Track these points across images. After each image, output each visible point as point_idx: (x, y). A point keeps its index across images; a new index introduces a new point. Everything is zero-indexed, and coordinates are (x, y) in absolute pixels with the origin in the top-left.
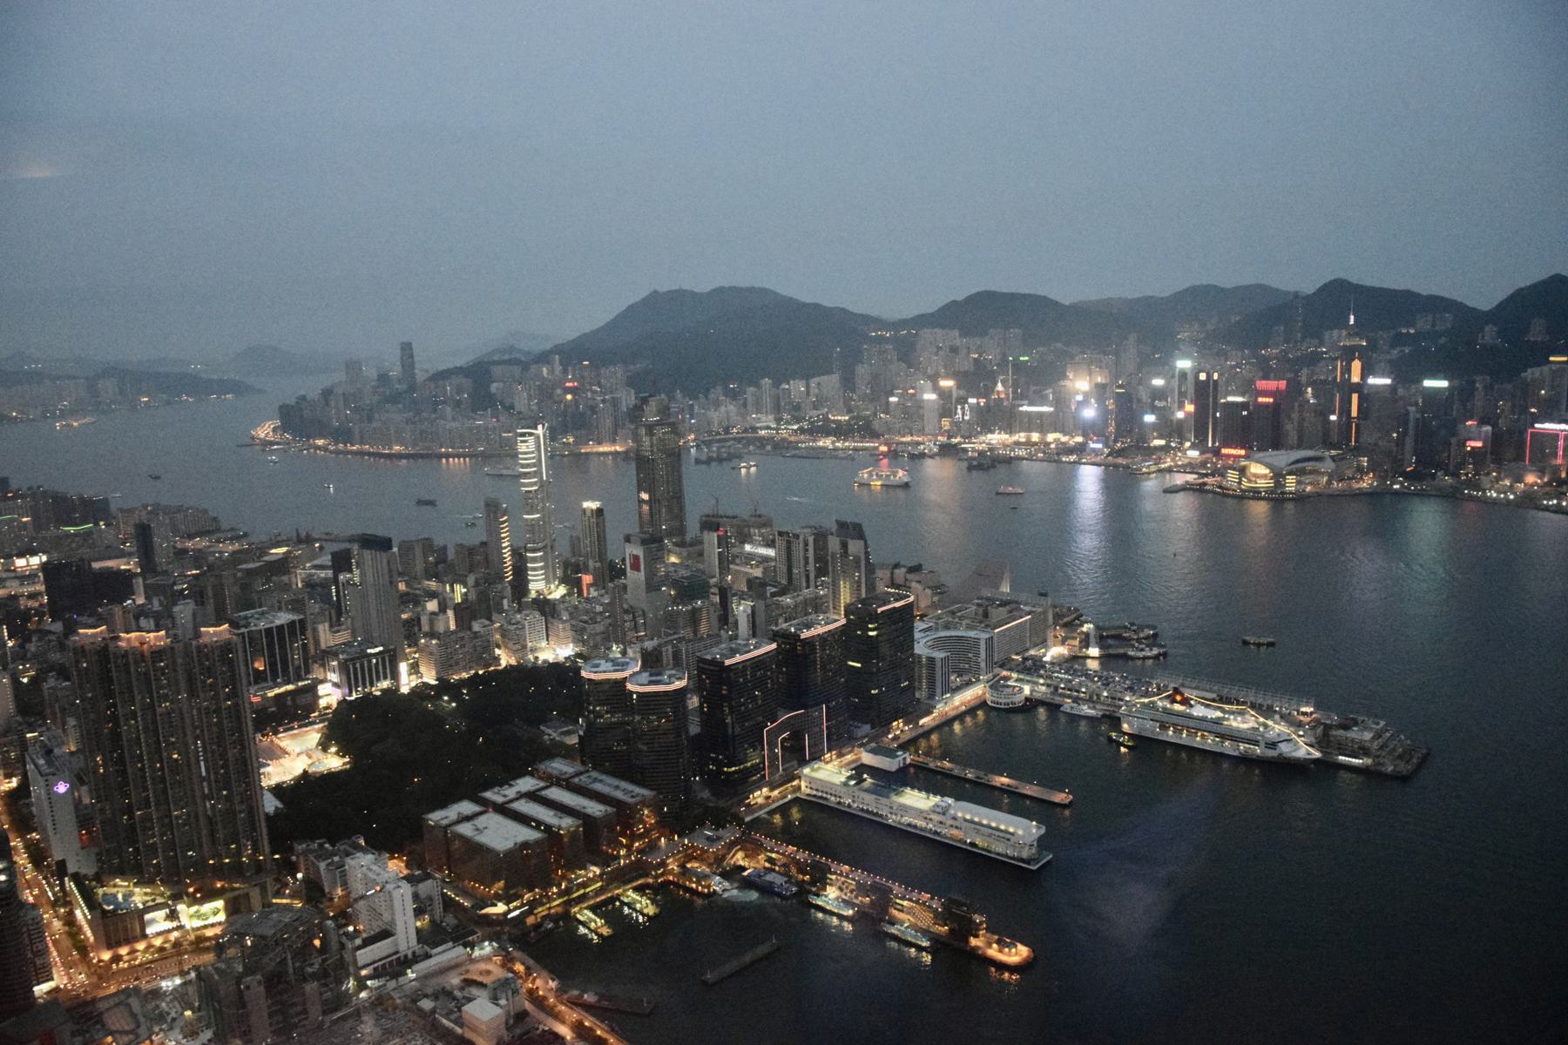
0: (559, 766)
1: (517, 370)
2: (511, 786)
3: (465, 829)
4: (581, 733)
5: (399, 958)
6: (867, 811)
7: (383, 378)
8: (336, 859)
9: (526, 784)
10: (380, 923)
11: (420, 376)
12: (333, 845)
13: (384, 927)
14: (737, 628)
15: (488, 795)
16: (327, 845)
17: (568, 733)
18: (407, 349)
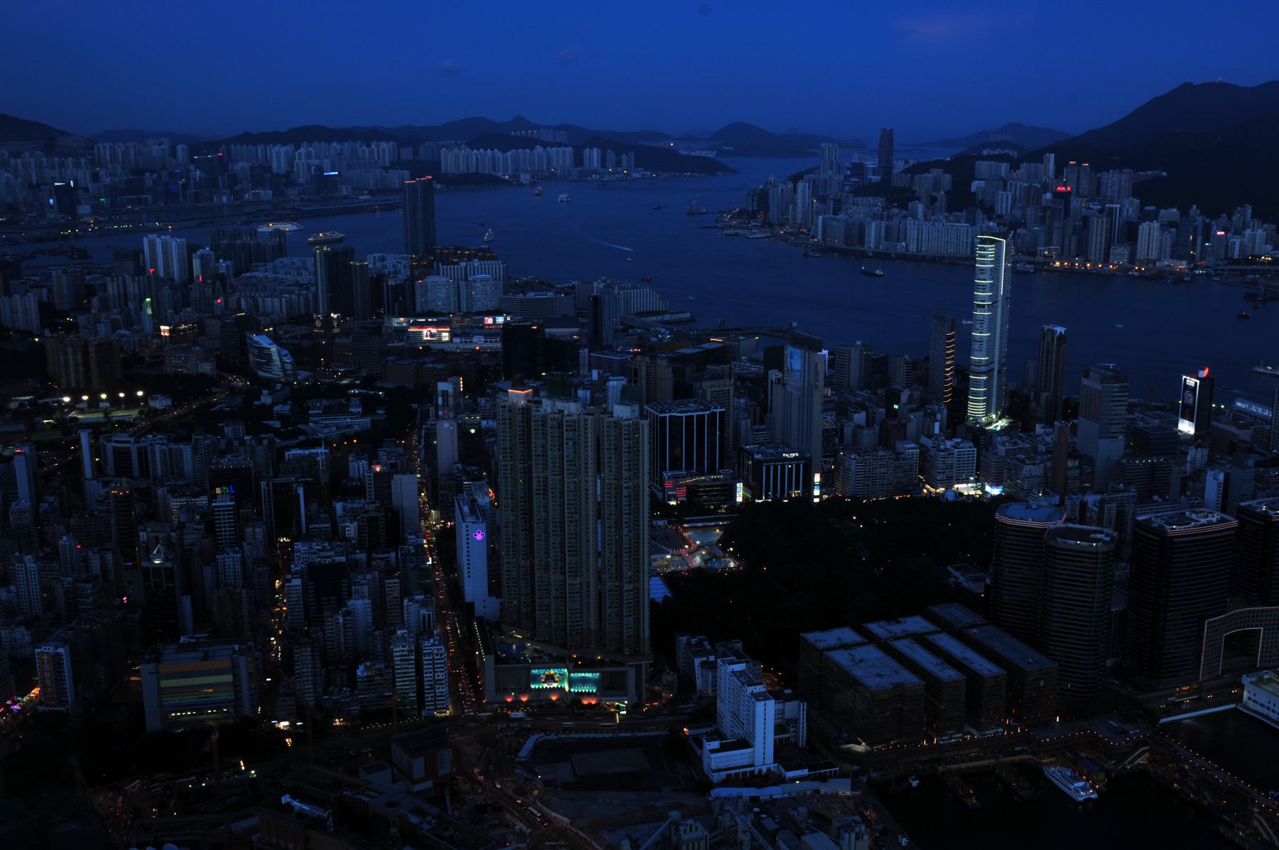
0: (956, 613)
1: (1004, 167)
2: (899, 622)
3: (841, 657)
4: (988, 581)
5: (754, 771)
7: (858, 169)
8: (712, 658)
9: (916, 624)
10: (741, 732)
11: (899, 166)
12: (712, 644)
13: (743, 736)
15: (875, 627)
16: (706, 643)
18: (887, 137)
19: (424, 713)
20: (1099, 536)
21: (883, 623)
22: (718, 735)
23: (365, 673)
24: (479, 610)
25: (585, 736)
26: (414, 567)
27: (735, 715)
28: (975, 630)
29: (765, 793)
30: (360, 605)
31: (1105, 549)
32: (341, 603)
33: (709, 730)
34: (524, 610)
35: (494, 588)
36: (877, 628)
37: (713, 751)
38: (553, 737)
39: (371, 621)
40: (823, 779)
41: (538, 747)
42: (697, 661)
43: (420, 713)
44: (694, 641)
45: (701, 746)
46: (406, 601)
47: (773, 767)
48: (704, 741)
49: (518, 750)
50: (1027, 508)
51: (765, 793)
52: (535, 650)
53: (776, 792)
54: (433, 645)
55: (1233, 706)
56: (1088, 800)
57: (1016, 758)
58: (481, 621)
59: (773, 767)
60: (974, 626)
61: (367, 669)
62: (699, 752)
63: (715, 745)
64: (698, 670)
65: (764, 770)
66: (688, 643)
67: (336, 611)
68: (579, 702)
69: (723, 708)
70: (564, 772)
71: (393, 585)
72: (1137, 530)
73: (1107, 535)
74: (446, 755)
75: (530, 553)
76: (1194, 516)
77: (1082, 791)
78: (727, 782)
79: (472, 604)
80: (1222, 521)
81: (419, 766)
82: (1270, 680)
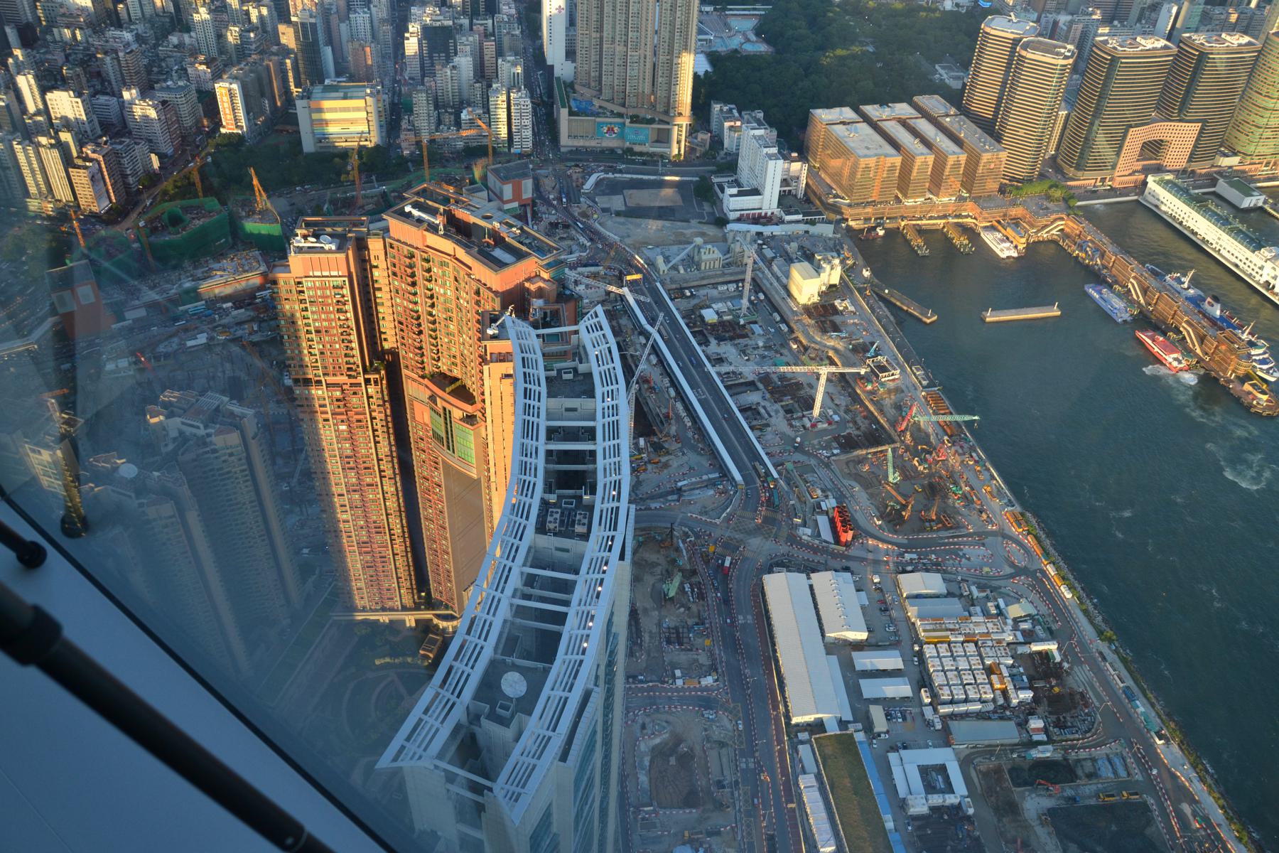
0: (934, 103)
4: (965, 80)
5: (760, 214)
6: (1196, 234)
8: (738, 123)
9: (903, 109)
10: (755, 183)
14: (1154, 26)
16: (735, 111)
17: (958, 78)
19: (512, 151)
20: (1062, 50)
21: (876, 106)
22: (737, 183)
23: (468, 117)
24: (557, 72)
25: (635, 176)
26: (508, 33)
27: (752, 170)
28: (948, 119)
29: (767, 230)
30: (465, 62)
31: (1065, 62)
32: (448, 59)
33: (730, 179)
34: (593, 74)
35: (570, 54)
36: (872, 110)
37: (732, 196)
38: (610, 175)
39: (471, 74)
40: (813, 223)
41: (598, 183)
42: (727, 124)
43: (509, 150)
44: (725, 109)
45: (723, 191)
46: (500, 61)
47: (777, 211)
48: (726, 189)
49: (583, 184)
50: (1009, 21)
51: (767, 230)
52: (600, 107)
53: (777, 230)
54: (521, 97)
55: (1136, 198)
56: (1008, 257)
57: (960, 220)
58: (558, 79)
59: (777, 211)
60: (947, 116)
61: (469, 113)
62: (721, 195)
63: (734, 191)
64: (726, 131)
65: (769, 214)
66: (721, 110)
67: (444, 66)
68: (632, 149)
69: (743, 164)
70: (617, 202)
71: (490, 47)
72: (1094, 49)
73: (1069, 51)
74: (528, 184)
75: (600, 29)
76: (1143, 42)
77: (1005, 251)
78: (739, 220)
79: (552, 67)
80: (1166, 47)
81: (508, 190)
82: (1168, 182)
